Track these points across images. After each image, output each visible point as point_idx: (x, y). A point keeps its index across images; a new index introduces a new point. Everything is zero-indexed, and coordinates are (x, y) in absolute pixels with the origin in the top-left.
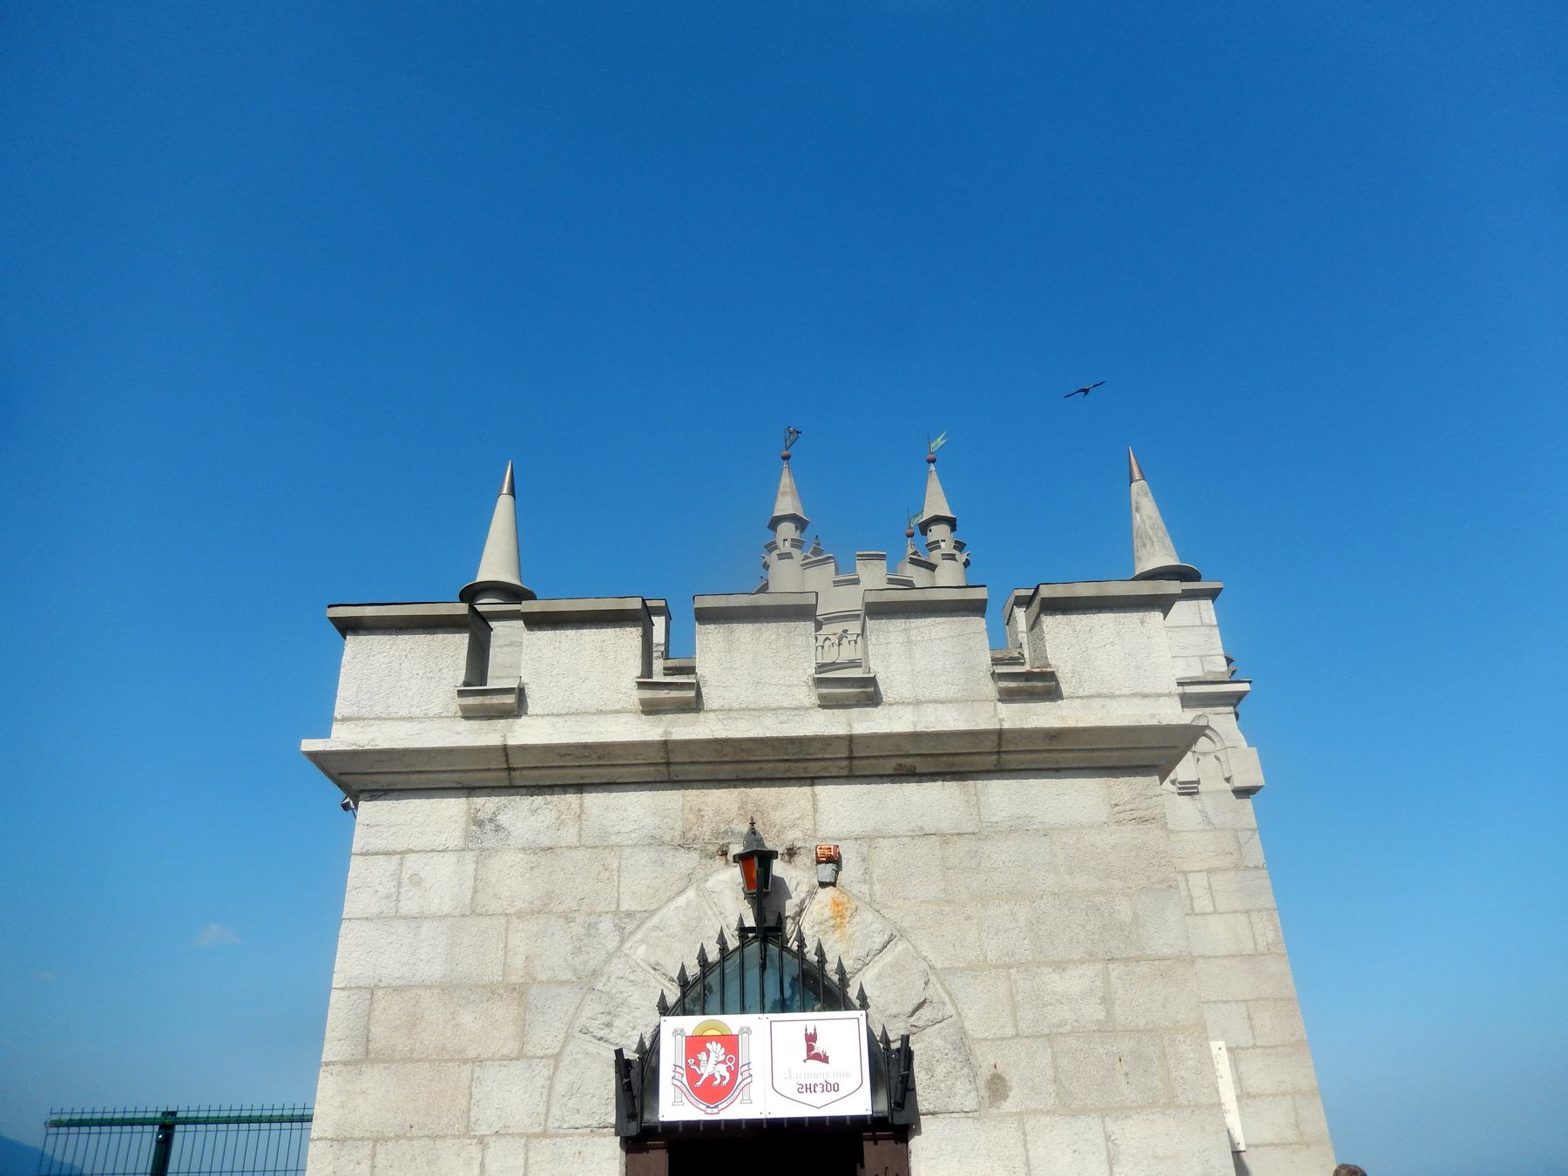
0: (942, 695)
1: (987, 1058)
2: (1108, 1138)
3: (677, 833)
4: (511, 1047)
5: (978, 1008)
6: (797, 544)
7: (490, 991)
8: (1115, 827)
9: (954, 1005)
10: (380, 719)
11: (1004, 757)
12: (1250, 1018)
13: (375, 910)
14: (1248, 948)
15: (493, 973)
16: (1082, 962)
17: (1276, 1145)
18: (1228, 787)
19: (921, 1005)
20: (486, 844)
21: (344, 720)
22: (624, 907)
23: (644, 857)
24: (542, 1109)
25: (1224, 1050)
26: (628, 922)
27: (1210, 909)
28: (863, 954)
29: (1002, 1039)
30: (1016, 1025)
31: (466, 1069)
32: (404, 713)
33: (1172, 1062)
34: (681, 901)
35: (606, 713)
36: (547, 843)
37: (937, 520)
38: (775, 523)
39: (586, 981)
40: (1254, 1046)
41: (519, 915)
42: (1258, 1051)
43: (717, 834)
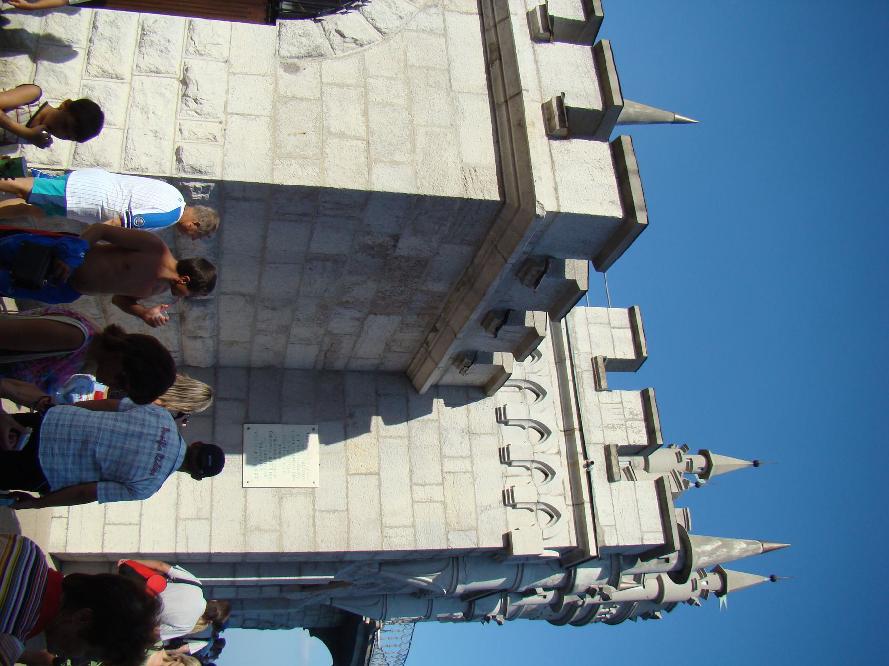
1: (310, 67)
2: (257, 116)
5: (340, 68)
6: (690, 465)
8: (459, 166)
9: (342, 58)
11: (504, 107)
12: (334, 511)
14: (387, 521)
16: (368, 126)
17: (245, 511)
18: (511, 529)
19: (343, 36)
27: (416, 498)
28: (374, 17)
29: (320, 76)
30: (329, 84)
37: (724, 578)
38: (704, 453)
40: (314, 510)
42: (311, 513)
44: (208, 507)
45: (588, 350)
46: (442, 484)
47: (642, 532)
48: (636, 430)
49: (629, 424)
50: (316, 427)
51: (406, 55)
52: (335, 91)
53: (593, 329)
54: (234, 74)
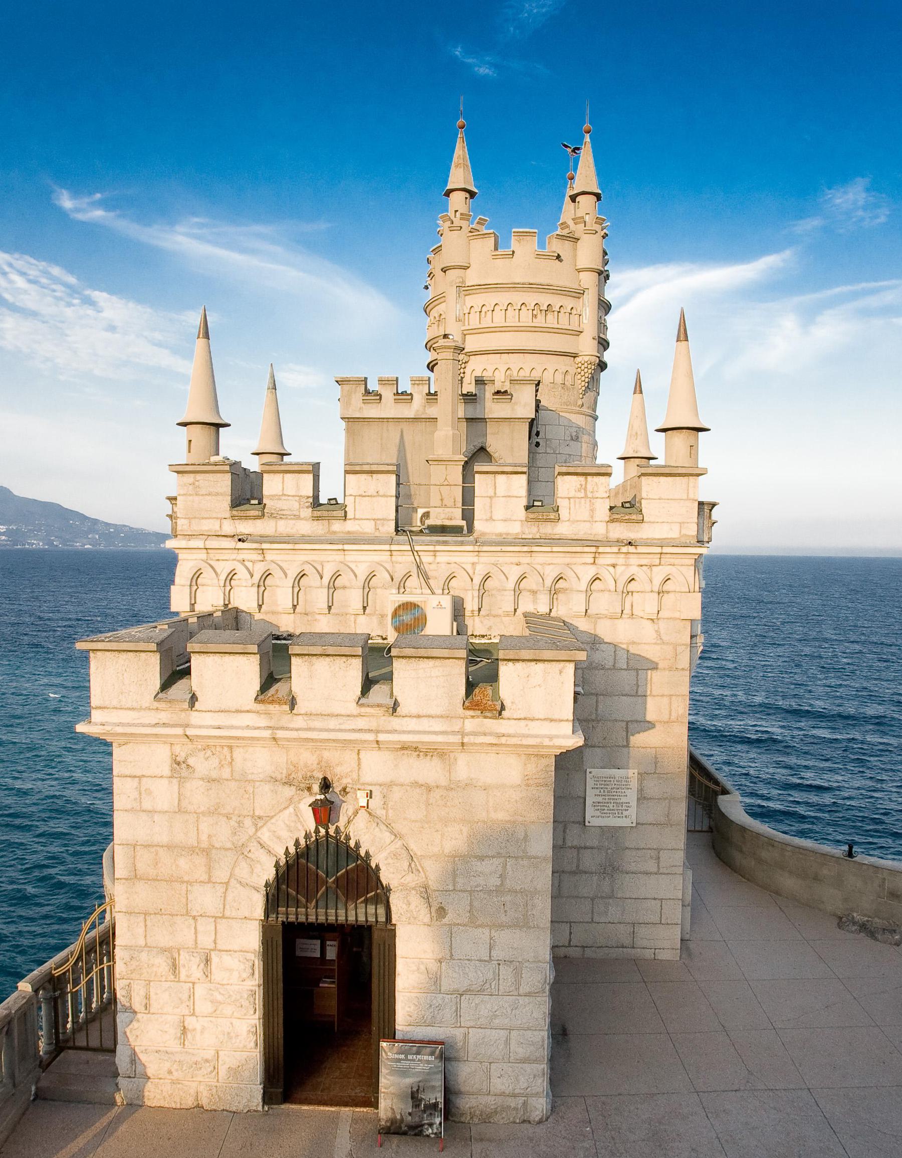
0: (433, 713)
2: (491, 939)
3: (284, 776)
4: (205, 877)
7: (192, 850)
10: (116, 708)
13: (129, 807)
15: (193, 841)
16: (493, 857)
20: (183, 775)
21: (96, 708)
22: (257, 813)
23: (267, 787)
24: (221, 906)
25: (636, 774)
26: (259, 820)
30: (454, 886)
31: (184, 886)
32: (129, 705)
33: (529, 907)
34: (287, 812)
35: (241, 712)
36: (214, 775)
38: (448, 193)
39: (241, 851)
41: (203, 813)
43: (305, 778)
44: (650, 851)
45: (518, 524)
46: (637, 670)
47: (688, 499)
48: (596, 488)
49: (590, 495)
50: (588, 770)
51: (416, 821)
52: (460, 881)
53: (498, 514)
54: (452, 955)
